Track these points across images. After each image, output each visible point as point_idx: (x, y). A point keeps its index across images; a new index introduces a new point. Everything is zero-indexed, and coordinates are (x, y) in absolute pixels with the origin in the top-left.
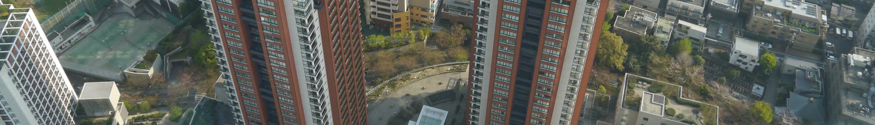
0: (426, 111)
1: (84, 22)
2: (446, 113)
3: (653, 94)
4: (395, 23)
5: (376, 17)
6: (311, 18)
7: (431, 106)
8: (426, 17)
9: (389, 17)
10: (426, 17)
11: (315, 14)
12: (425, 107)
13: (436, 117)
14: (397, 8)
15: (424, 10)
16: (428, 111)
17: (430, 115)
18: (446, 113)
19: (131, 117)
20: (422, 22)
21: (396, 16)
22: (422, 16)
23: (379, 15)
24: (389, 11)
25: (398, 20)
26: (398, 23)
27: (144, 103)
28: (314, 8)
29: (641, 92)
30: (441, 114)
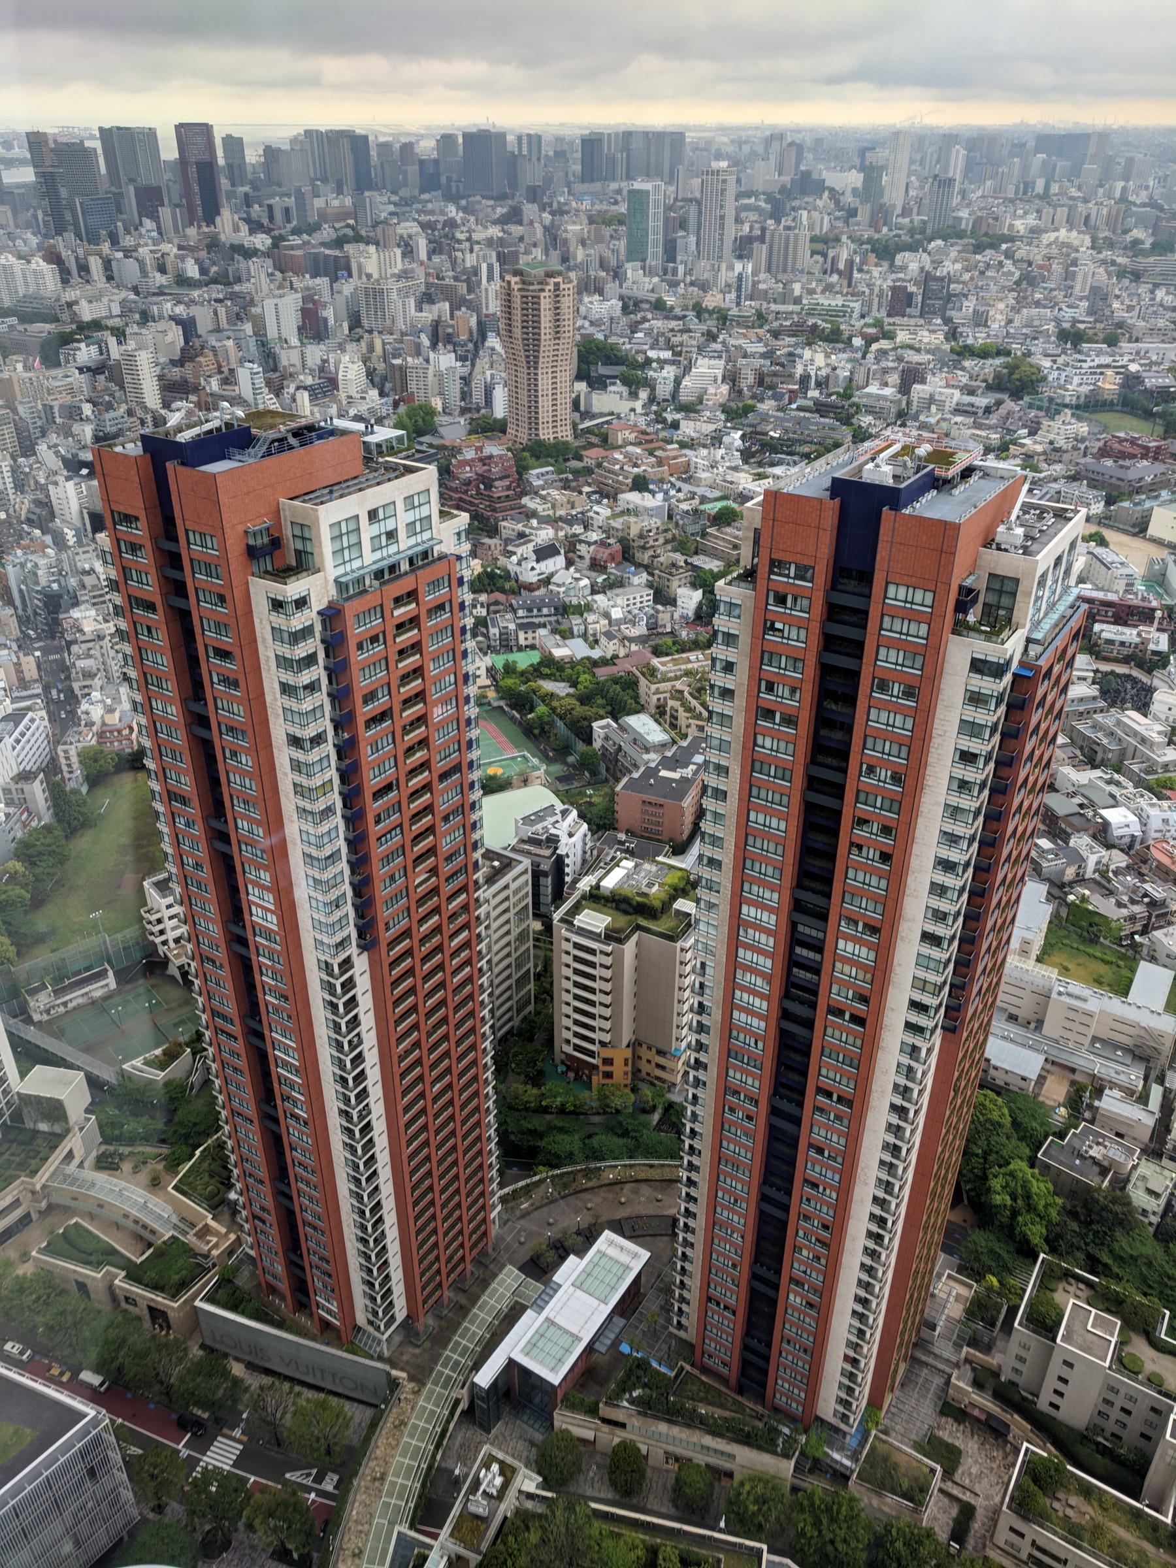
0: (608, 1241)
1: (102, 975)
2: (645, 1255)
3: (1094, 1311)
4: (602, 1068)
5: (569, 1049)
6: (347, 964)
7: (624, 1236)
8: (663, 1068)
9: (591, 1054)
10: (663, 1068)
11: (361, 963)
12: (607, 1234)
13: (625, 1259)
14: (606, 1038)
15: (660, 1053)
16: (611, 1243)
17: (612, 1252)
18: (645, 1255)
19: (103, 1148)
20: (657, 1078)
21: (607, 1053)
22: (658, 1066)
23: (577, 1048)
24: (592, 1041)
25: (608, 1061)
26: (608, 1068)
27: (132, 1126)
28: (358, 946)
29: (1070, 1301)
30: (636, 1256)
